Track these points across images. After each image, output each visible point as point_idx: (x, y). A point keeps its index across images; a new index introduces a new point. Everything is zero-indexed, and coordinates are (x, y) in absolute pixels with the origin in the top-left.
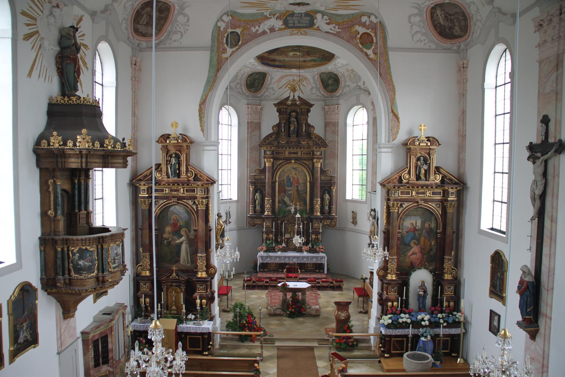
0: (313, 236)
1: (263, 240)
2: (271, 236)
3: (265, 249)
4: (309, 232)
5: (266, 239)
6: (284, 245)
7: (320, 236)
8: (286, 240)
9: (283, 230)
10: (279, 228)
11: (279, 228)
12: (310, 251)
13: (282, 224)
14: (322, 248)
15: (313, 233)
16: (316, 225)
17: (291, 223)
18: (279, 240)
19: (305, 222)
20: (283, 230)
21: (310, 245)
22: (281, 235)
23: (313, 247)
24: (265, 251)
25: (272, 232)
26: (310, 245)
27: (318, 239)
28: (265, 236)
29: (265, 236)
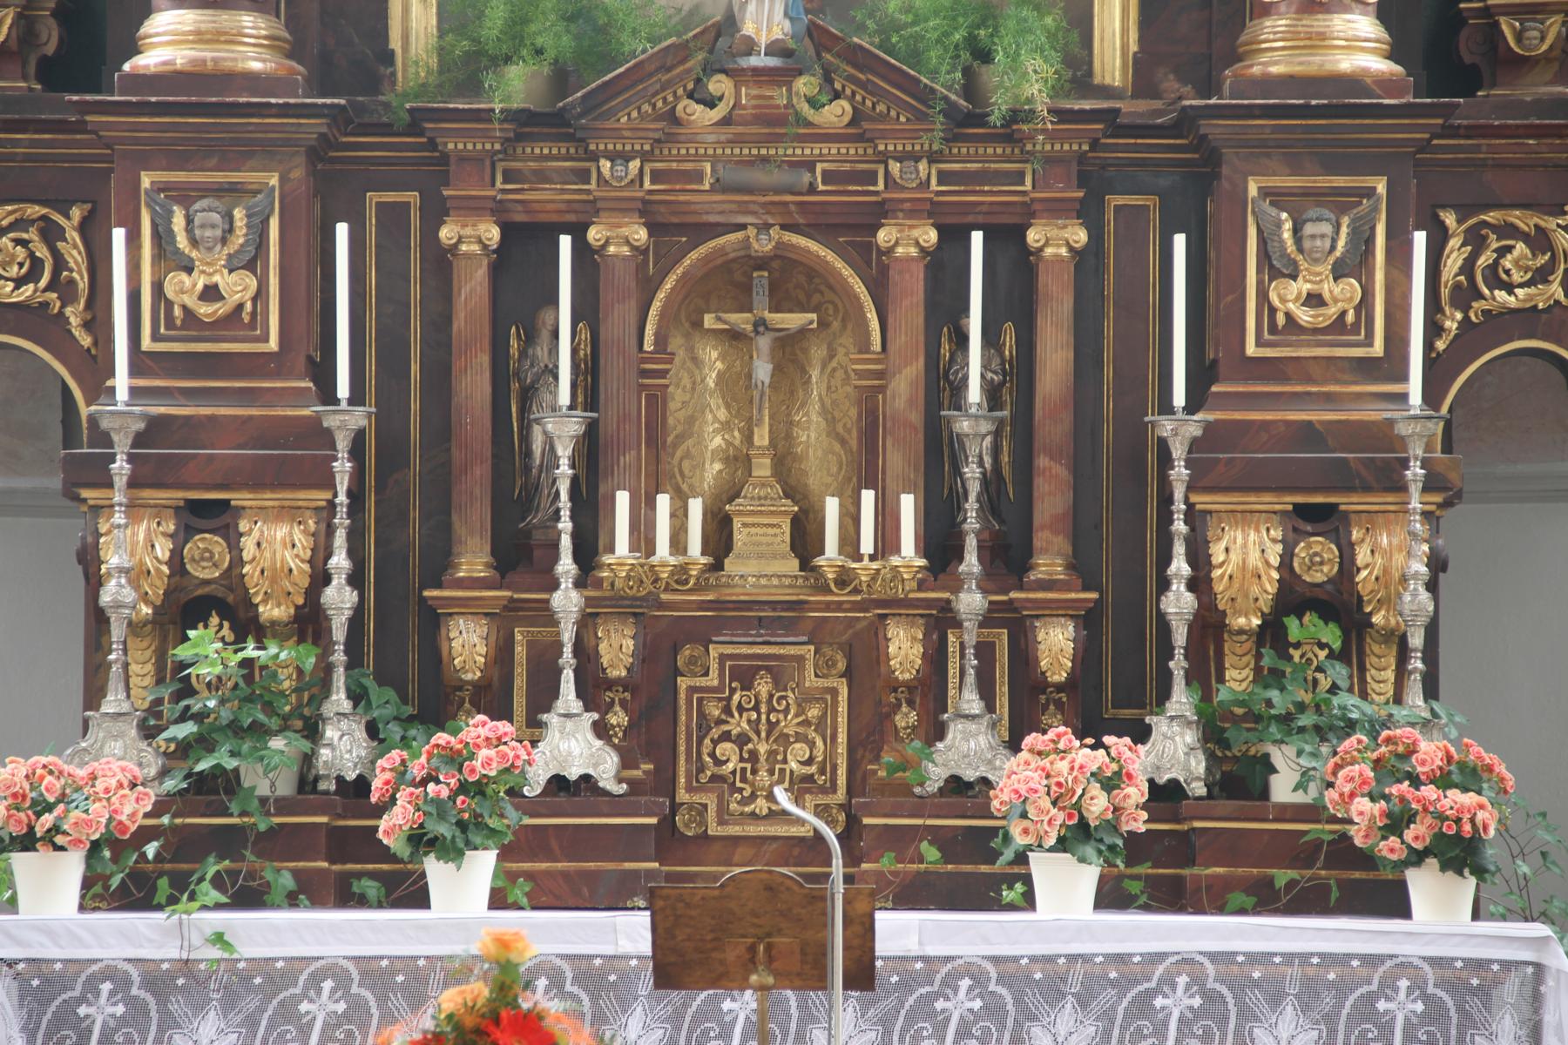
0: (1248, 552)
1: (98, 619)
2: (274, 545)
3: (118, 774)
4: (1141, 460)
5: (184, 607)
6: (573, 745)
7: (1391, 554)
8: (618, 649)
9: (559, 429)
10: (474, 384)
11: (474, 384)
12: (1159, 863)
13: (524, 249)
14: (1470, 776)
15: (1229, 464)
16: (1288, 295)
17: (731, 281)
18: (467, 644)
19: (1056, 240)
20: (559, 429)
21: (1174, 747)
22: (520, 556)
23: (1240, 779)
24: (127, 877)
25: (291, 461)
26: (1174, 747)
27: (1341, 605)
28: (135, 546)
29: (135, 546)
